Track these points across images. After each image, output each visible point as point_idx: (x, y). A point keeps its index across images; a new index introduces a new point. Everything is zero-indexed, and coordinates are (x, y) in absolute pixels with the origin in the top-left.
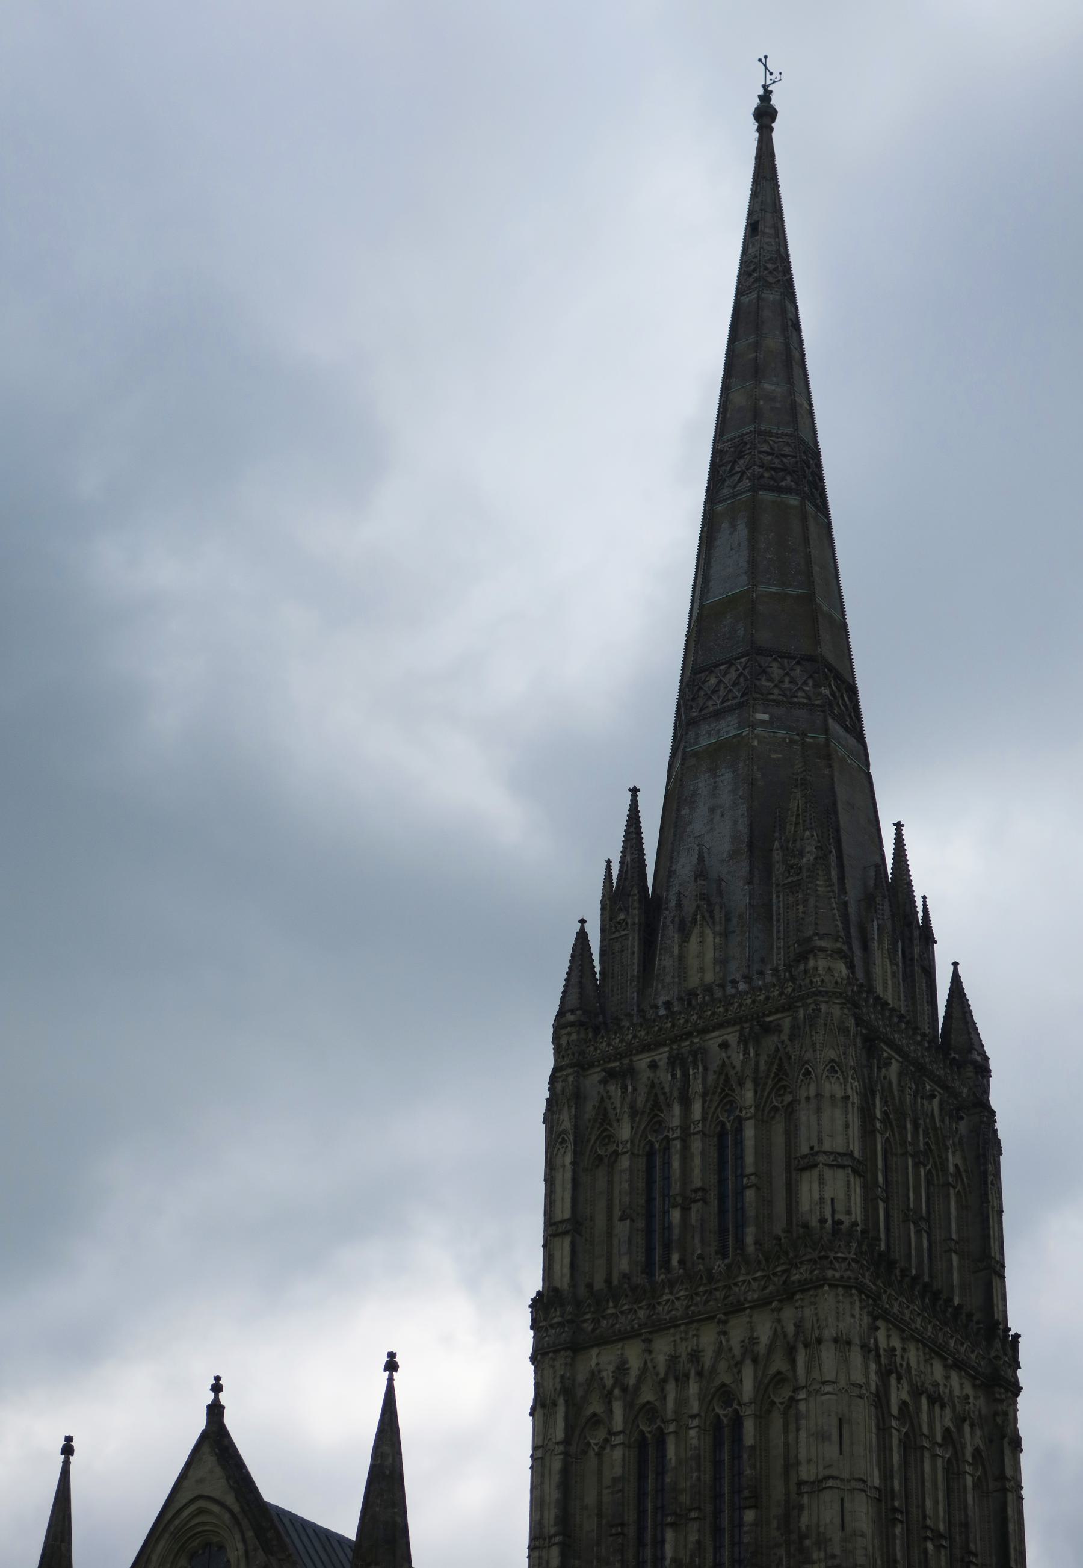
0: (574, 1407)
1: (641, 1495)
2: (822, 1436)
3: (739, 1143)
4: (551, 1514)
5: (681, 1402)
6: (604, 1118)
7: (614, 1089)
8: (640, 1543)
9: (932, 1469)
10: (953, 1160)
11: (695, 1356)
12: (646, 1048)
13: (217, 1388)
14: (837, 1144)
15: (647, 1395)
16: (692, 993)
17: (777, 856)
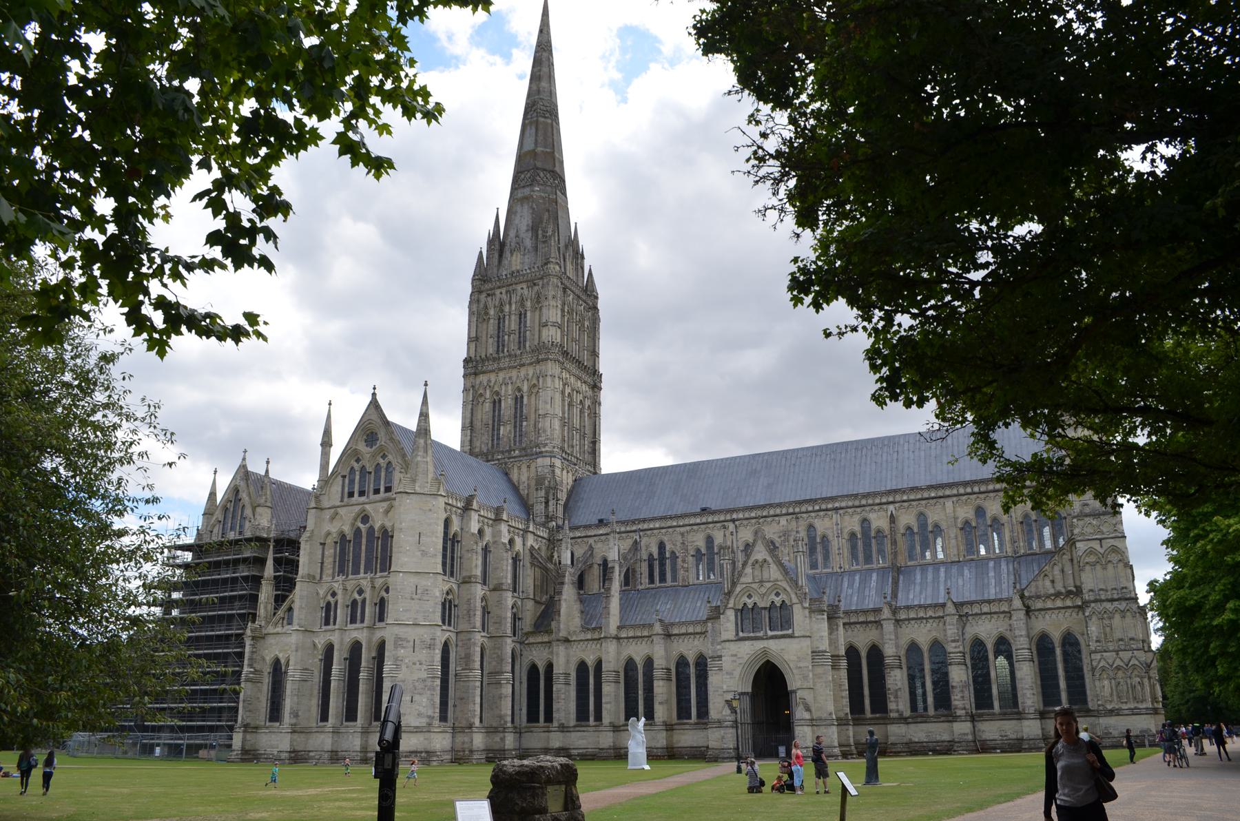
0: (475, 391)
1: (494, 416)
2: (546, 403)
3: (525, 317)
4: (468, 421)
5: (506, 391)
6: (486, 307)
7: (489, 299)
8: (493, 430)
9: (576, 411)
10: (587, 323)
11: (510, 378)
12: (499, 288)
13: (374, 388)
14: (553, 319)
15: (496, 388)
16: (513, 272)
17: (540, 232)
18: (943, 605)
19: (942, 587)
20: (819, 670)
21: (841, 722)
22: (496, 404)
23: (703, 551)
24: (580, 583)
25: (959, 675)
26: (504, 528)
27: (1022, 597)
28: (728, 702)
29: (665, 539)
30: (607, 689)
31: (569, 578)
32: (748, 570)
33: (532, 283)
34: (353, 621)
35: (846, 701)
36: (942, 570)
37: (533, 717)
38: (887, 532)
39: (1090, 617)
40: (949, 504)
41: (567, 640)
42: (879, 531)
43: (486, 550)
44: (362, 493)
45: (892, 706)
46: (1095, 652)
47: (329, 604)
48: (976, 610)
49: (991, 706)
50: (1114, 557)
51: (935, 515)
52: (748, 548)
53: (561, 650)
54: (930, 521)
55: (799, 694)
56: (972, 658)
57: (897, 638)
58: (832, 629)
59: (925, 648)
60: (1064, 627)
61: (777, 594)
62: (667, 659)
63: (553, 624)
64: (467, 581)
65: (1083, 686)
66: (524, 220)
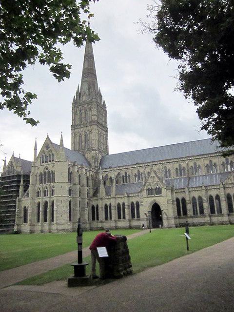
9: (102, 138)
14: (96, 114)
19: (201, 182)
20: (169, 205)
21: (175, 218)
22: (80, 137)
24: (105, 184)
25: (206, 205)
26: (84, 170)
27: (223, 184)
28: (145, 214)
29: (127, 171)
30: (112, 211)
31: (102, 183)
32: (150, 179)
33: (89, 104)
34: (45, 196)
35: (176, 213)
37: (93, 219)
38: (186, 168)
41: (102, 199)
43: (79, 176)
44: (46, 162)
45: (188, 214)
47: (38, 192)
48: (210, 188)
49: (215, 213)
51: (199, 163)
52: (149, 173)
53: (100, 201)
54: (197, 165)
55: (164, 211)
56: (210, 201)
58: (172, 194)
62: (128, 202)
64: (75, 184)
66: (86, 87)
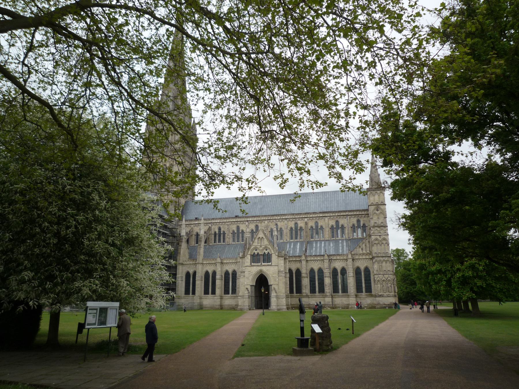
18: (323, 256)
19: (323, 249)
20: (280, 278)
23: (236, 232)
25: (328, 281)
27: (352, 255)
29: (221, 226)
31: (184, 240)
35: (288, 289)
36: (323, 243)
39: (375, 262)
40: (326, 219)
42: (301, 228)
46: (376, 275)
48: (335, 258)
49: (338, 292)
50: (384, 242)
51: (321, 223)
54: (319, 225)
56: (333, 275)
57: (306, 266)
58: (285, 263)
59: (316, 271)
60: (365, 265)
61: (266, 250)
62: (221, 271)
63: (178, 258)
65: (371, 286)
